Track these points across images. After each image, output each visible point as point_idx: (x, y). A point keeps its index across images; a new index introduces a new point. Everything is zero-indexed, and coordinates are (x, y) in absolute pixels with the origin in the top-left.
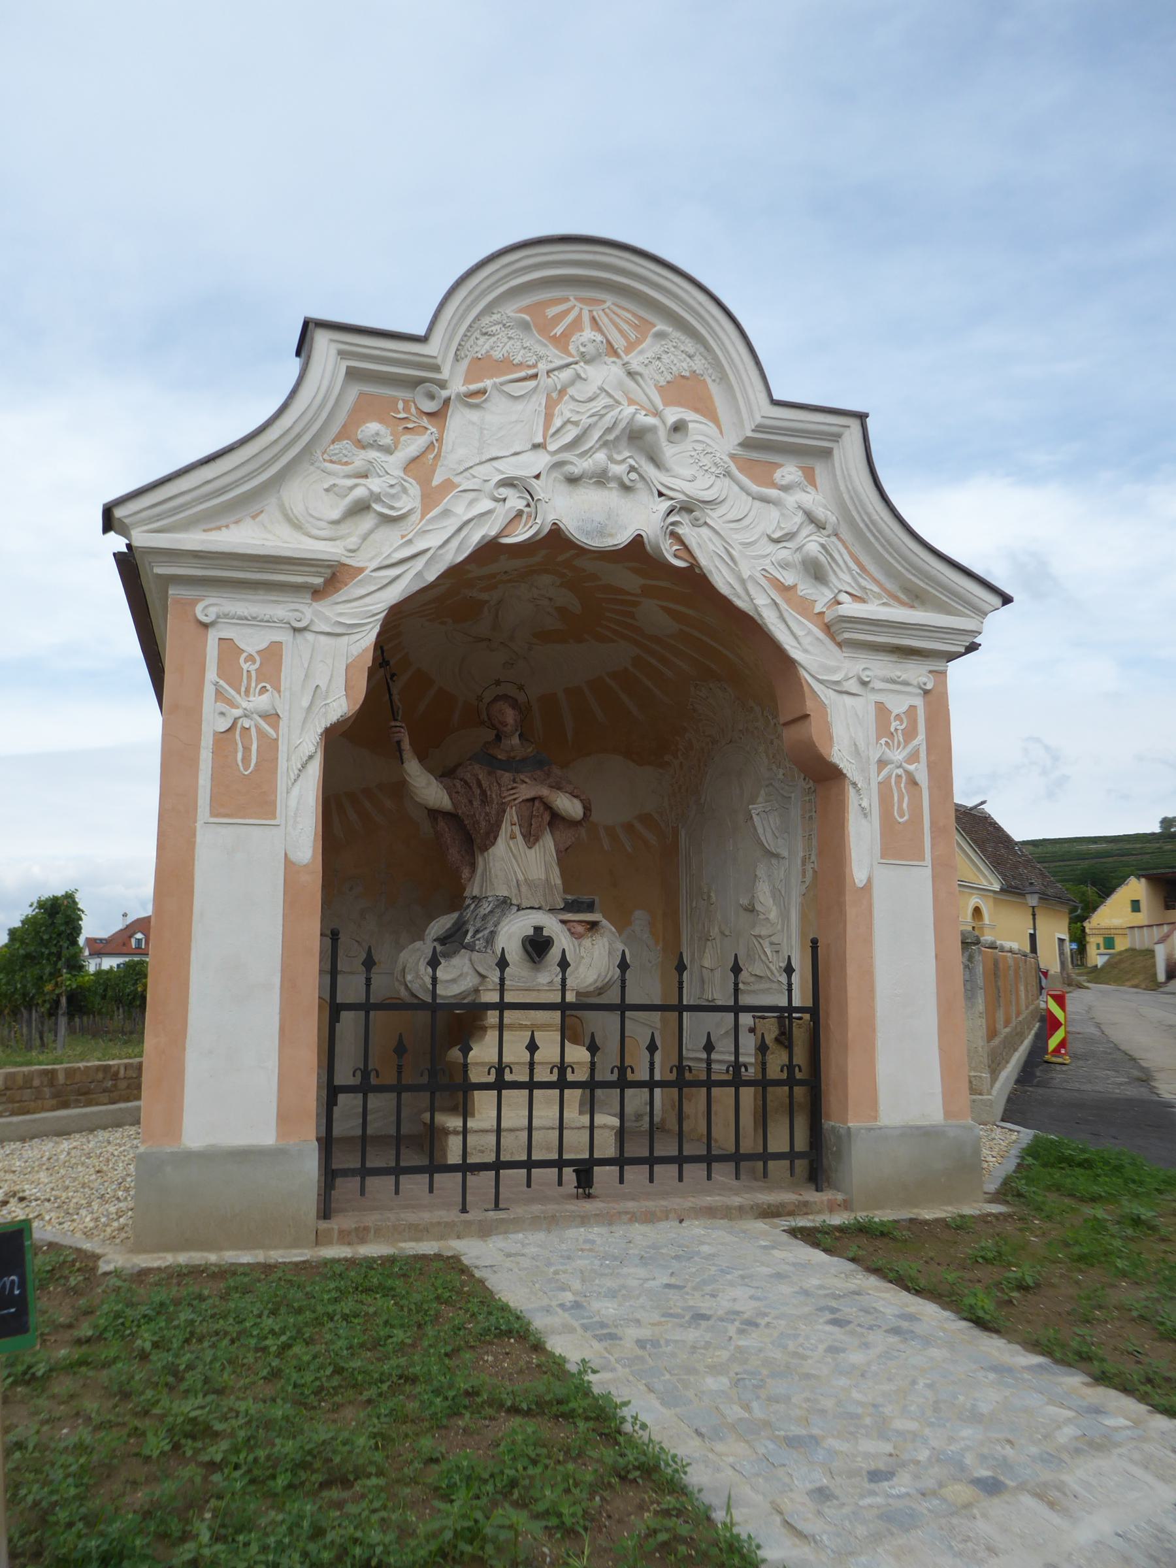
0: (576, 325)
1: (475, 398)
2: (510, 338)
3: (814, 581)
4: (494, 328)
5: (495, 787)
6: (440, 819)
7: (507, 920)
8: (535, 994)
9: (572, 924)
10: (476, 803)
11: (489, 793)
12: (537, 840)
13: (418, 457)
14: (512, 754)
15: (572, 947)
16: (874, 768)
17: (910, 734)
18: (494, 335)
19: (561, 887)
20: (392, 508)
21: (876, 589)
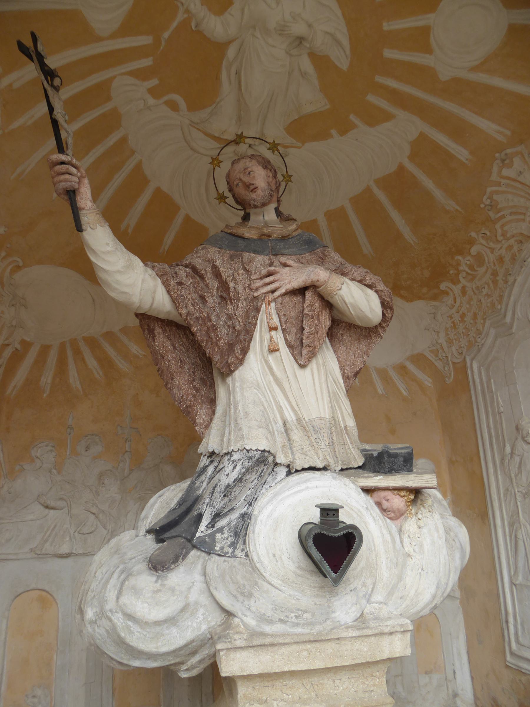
5: (242, 276)
6: (158, 331)
7: (272, 491)
8: (330, 648)
9: (383, 494)
10: (212, 301)
11: (232, 285)
12: (313, 354)
14: (266, 231)
15: (387, 537)
19: (354, 431)
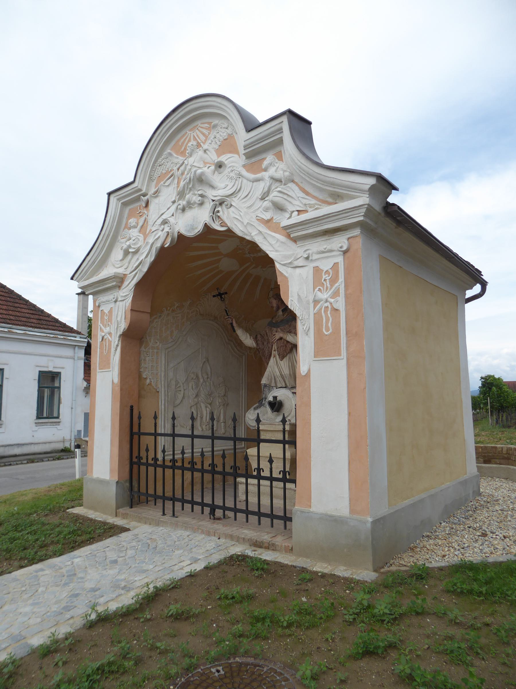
0: (189, 141)
1: (156, 194)
2: (167, 162)
3: (280, 212)
4: (162, 162)
8: (274, 426)
13: (143, 225)
16: (312, 305)
17: (334, 280)
18: (163, 164)
20: (134, 248)
21: (313, 201)
